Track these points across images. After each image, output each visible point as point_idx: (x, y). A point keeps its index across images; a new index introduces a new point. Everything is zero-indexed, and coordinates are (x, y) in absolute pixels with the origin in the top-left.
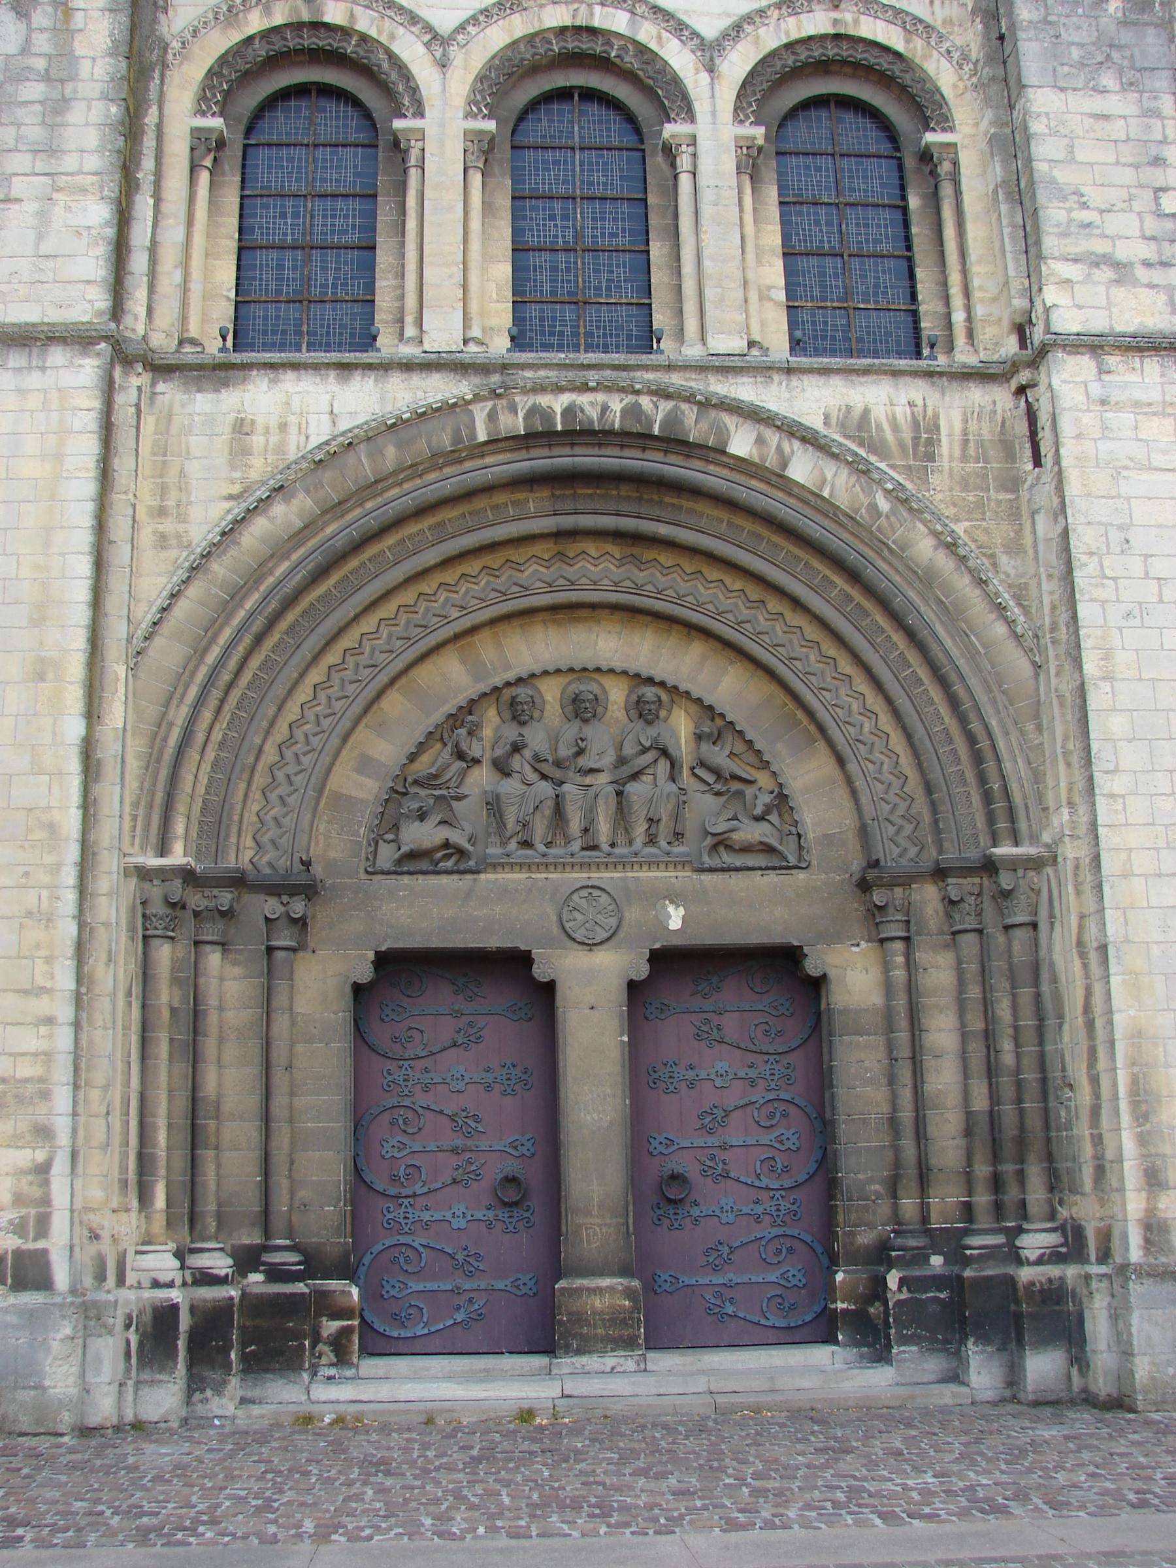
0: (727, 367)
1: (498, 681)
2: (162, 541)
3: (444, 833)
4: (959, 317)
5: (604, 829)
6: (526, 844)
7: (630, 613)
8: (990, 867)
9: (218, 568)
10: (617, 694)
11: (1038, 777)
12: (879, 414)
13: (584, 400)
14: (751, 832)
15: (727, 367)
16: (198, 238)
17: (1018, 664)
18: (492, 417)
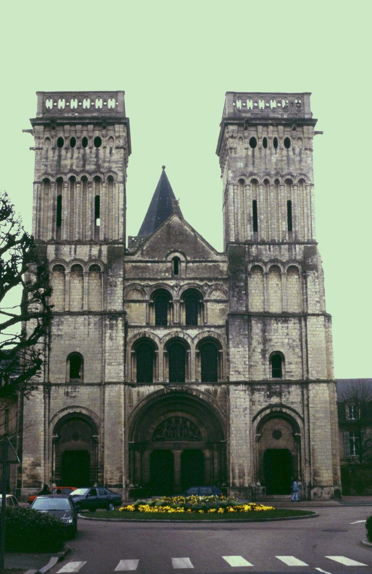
0: (193, 383)
1: (167, 418)
2: (130, 406)
3: (161, 436)
4: (221, 375)
5: (179, 436)
6: (170, 438)
7: (182, 411)
8: (220, 442)
9: (137, 409)
10: (181, 420)
11: (226, 433)
12: (211, 389)
13: (177, 388)
14: (196, 436)
15: (193, 383)
16: (132, 366)
17: (225, 419)
18: (167, 390)
